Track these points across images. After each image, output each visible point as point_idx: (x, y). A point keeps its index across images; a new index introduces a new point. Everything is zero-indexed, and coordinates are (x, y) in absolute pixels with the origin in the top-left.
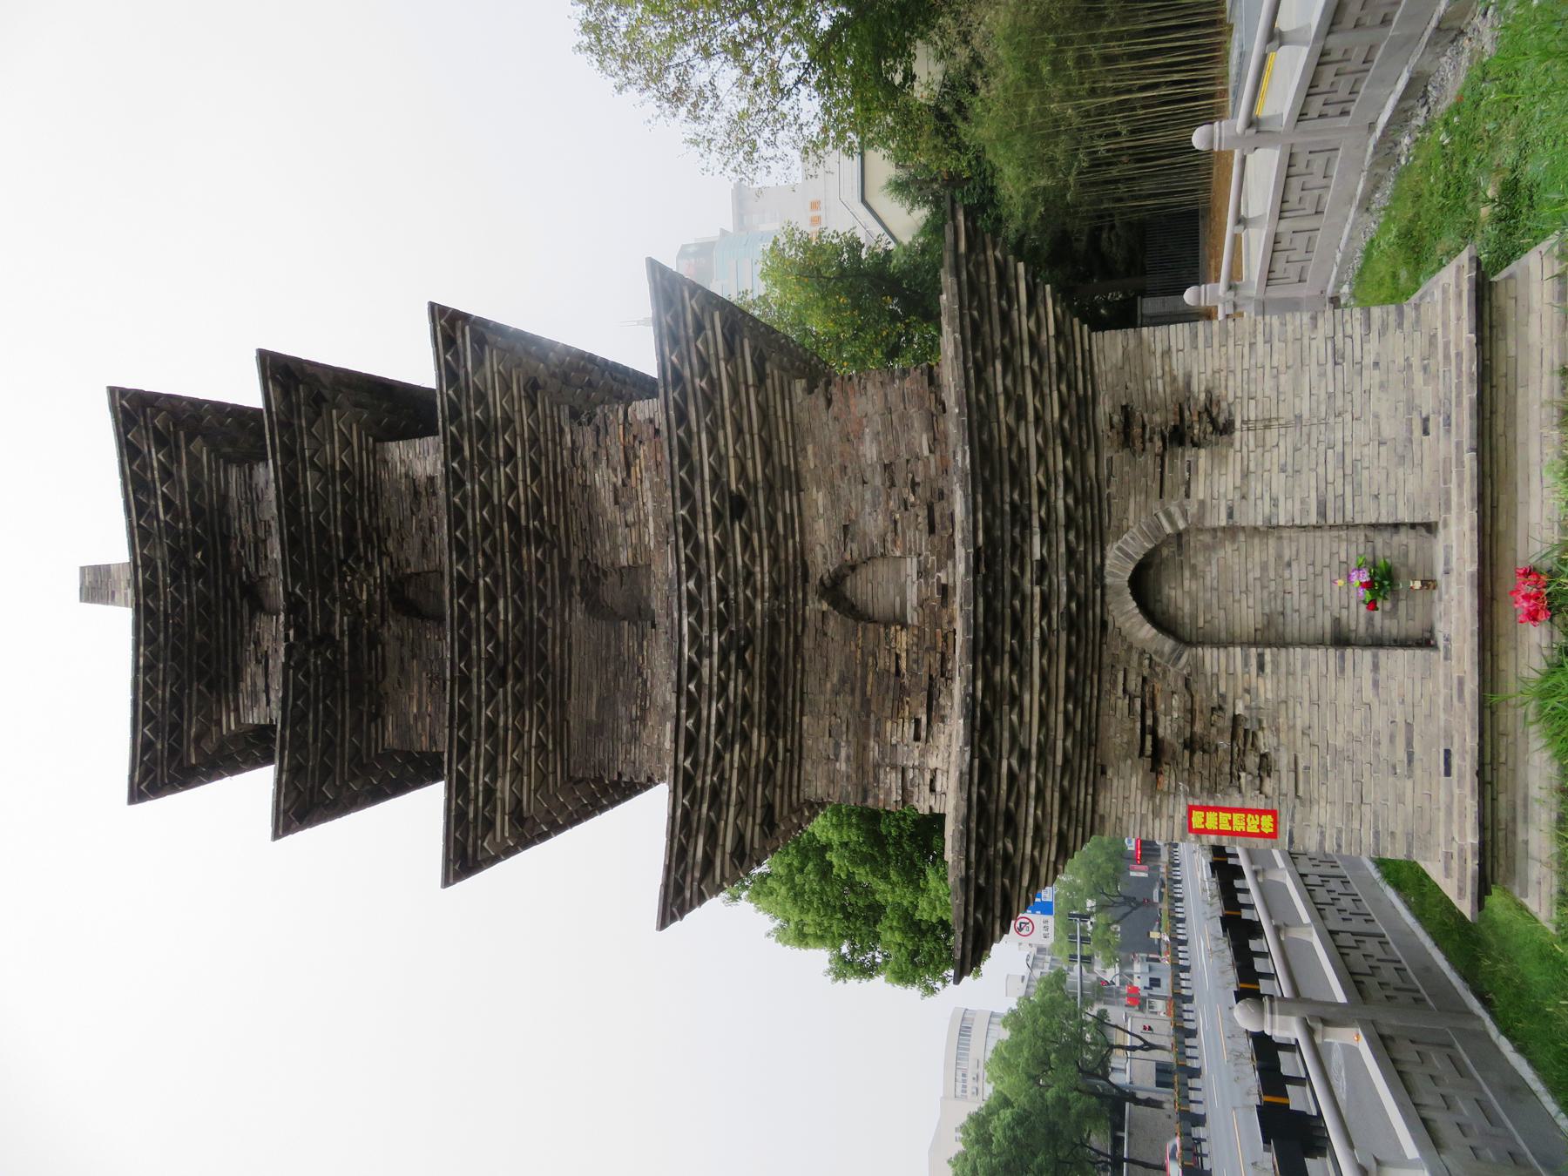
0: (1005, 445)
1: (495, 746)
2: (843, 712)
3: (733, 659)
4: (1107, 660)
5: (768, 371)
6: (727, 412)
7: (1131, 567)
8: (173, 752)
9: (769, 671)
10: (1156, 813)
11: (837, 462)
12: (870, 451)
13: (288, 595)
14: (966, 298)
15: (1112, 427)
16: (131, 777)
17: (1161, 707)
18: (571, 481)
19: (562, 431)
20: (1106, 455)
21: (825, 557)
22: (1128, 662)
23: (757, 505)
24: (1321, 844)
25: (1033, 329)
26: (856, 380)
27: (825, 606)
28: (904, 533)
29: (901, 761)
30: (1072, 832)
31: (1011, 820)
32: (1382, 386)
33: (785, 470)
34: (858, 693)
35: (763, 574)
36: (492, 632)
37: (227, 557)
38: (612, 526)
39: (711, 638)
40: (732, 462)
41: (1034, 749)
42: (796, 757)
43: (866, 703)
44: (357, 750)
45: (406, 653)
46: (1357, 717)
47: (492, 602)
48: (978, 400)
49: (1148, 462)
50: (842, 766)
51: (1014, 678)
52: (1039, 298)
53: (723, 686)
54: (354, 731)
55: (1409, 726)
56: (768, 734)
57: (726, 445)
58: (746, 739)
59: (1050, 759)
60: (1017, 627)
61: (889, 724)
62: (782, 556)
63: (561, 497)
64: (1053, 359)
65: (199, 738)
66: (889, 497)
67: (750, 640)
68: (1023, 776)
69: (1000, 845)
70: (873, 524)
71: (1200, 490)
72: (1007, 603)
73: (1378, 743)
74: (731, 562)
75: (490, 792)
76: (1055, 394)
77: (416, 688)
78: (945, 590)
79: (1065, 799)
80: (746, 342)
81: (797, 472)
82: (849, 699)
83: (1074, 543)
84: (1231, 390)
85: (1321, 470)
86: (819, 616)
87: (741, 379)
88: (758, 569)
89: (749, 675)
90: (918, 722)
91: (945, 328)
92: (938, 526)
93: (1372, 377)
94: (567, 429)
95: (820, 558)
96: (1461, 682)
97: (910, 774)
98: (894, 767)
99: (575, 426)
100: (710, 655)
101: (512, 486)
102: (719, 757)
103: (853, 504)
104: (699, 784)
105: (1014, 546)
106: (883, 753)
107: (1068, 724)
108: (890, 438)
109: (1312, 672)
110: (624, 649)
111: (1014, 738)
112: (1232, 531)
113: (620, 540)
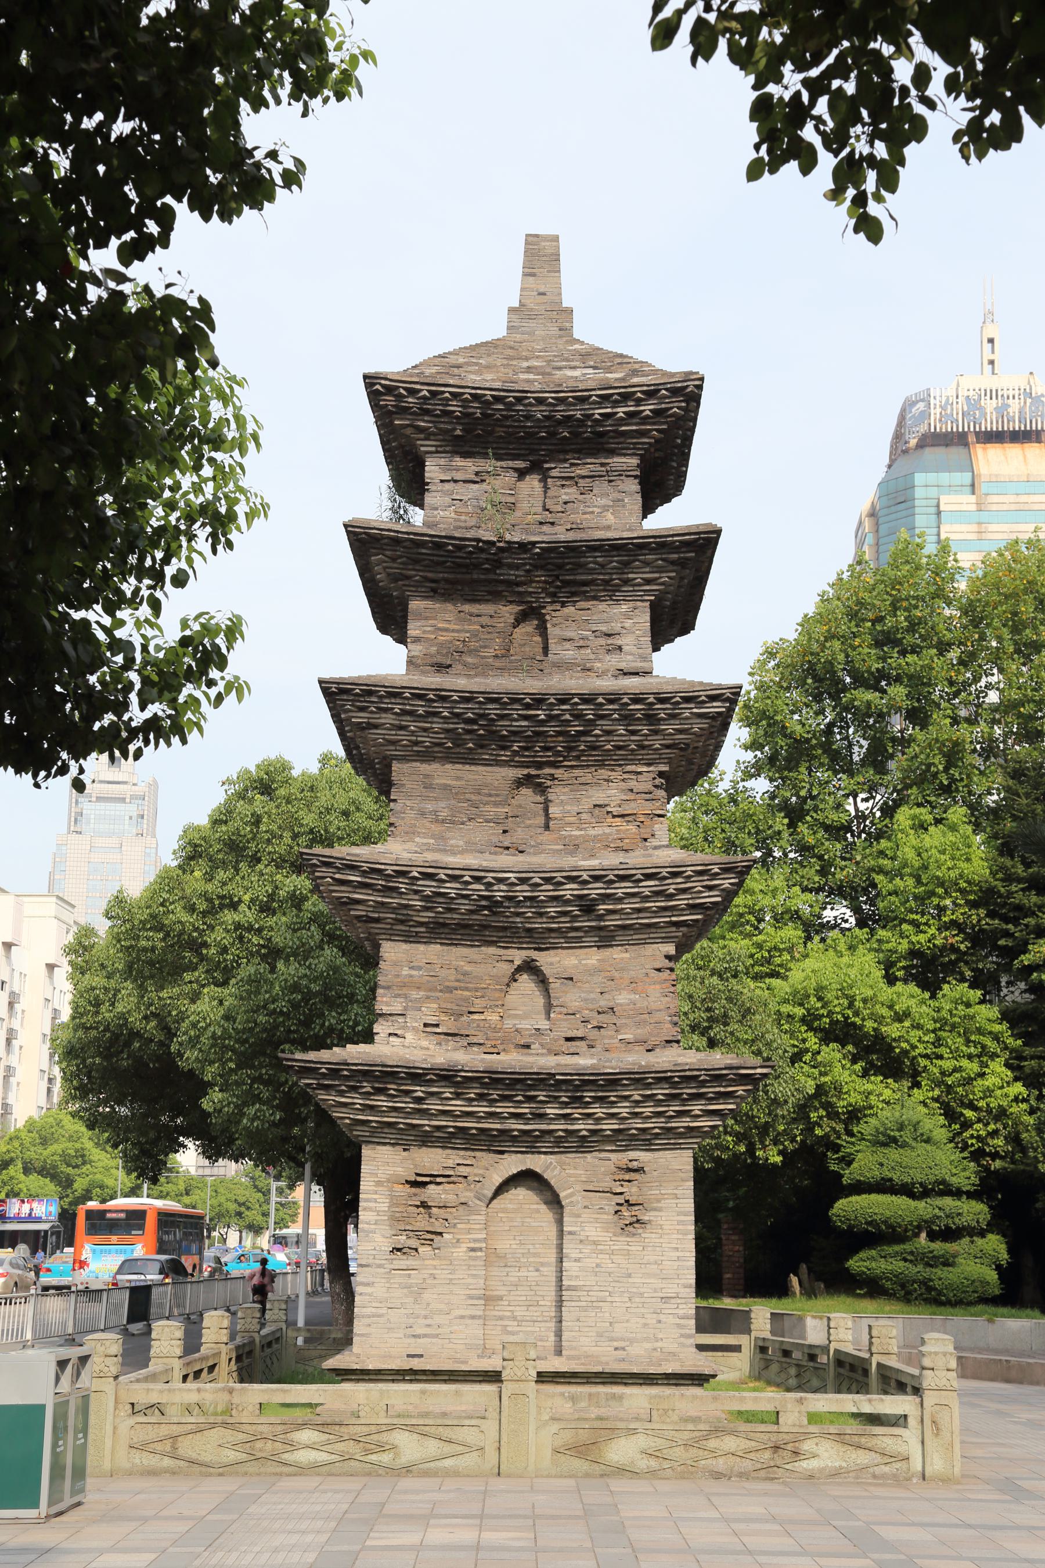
1: (420, 716)
3: (484, 903)
4: (478, 1154)
10: (379, 1183)
11: (616, 974)
12: (622, 998)
13: (534, 543)
16: (386, 379)
17: (447, 1187)
18: (613, 770)
19: (649, 765)
20: (613, 1156)
21: (552, 964)
26: (672, 989)
27: (517, 962)
31: (379, 1091)
32: (645, 1325)
34: (457, 984)
36: (502, 717)
37: (566, 452)
42: (410, 938)
43: (450, 990)
44: (408, 578)
45: (485, 620)
46: (442, 1306)
47: (526, 718)
49: (607, 1183)
50: (406, 971)
55: (437, 1336)
60: (504, 1098)
61: (436, 1006)
63: (601, 764)
65: (417, 428)
67: (495, 914)
71: (586, 1215)
73: (426, 1317)
77: (456, 627)
78: (528, 1047)
79: (390, 1125)
80: (699, 917)
81: (612, 946)
82: (452, 978)
84: (648, 1235)
85: (596, 1288)
89: (471, 912)
90: (437, 1026)
91: (701, 1055)
93: (651, 1319)
94: (651, 769)
95: (550, 960)
96: (465, 1362)
97: (401, 1019)
98: (406, 1008)
99: (653, 775)
100: (486, 890)
101: (608, 733)
102: (416, 892)
107: (438, 1128)
109: (471, 1281)
110: (488, 808)
112: (561, 1233)
113: (568, 808)
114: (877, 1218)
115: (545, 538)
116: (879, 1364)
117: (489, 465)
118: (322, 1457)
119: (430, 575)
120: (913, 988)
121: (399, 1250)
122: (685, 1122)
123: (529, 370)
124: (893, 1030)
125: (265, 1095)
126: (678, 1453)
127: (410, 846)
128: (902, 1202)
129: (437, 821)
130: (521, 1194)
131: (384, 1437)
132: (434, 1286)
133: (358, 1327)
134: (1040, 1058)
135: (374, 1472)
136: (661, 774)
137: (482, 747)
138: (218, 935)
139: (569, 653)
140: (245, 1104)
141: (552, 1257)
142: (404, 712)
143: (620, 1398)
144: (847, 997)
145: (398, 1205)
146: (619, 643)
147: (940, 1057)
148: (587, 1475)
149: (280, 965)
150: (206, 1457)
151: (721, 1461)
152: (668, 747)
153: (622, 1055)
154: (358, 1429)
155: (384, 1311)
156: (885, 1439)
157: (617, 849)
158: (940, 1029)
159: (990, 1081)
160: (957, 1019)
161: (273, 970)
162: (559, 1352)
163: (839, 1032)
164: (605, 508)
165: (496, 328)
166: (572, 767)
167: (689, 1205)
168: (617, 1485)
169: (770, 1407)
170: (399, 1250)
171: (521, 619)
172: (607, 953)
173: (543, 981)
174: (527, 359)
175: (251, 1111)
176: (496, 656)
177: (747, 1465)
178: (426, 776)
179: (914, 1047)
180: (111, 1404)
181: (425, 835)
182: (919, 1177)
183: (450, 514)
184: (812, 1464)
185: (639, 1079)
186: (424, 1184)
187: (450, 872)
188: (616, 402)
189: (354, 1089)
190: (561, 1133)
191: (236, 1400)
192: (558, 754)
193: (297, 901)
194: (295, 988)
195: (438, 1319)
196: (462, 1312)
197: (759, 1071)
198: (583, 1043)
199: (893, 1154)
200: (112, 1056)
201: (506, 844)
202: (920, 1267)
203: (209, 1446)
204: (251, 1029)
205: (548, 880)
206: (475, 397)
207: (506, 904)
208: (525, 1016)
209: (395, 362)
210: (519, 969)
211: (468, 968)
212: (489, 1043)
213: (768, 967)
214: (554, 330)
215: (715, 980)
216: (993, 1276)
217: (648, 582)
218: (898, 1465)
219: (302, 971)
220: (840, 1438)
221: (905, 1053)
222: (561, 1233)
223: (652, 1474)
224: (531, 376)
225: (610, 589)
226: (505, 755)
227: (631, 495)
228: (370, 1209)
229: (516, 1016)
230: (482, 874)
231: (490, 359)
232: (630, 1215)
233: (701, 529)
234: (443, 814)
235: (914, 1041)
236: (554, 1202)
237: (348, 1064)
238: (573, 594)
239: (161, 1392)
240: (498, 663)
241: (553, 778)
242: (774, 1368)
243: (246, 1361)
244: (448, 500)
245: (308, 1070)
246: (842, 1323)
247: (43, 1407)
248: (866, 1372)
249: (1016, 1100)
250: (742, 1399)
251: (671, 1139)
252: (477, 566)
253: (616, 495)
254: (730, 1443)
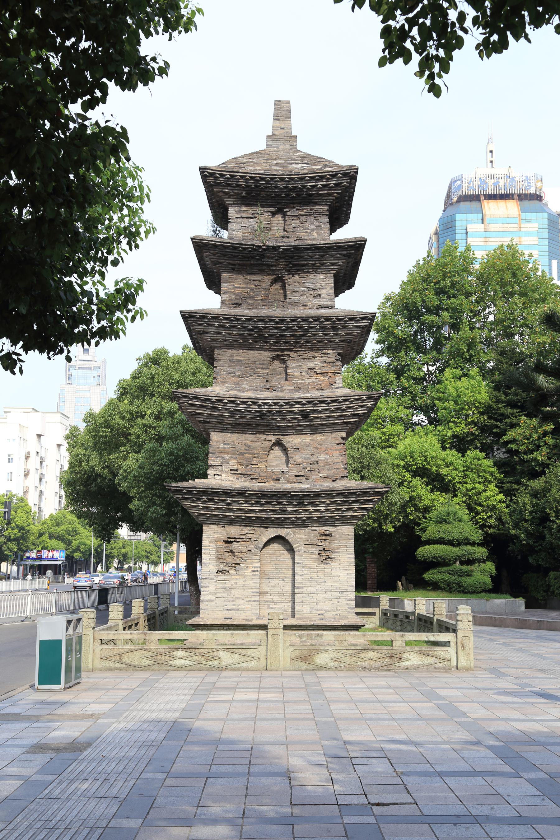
2: (239, 446)
3: (257, 414)
4: (256, 528)
8: (218, 184)
10: (211, 542)
11: (319, 446)
12: (322, 457)
19: (333, 350)
20: (317, 529)
24: (204, 587)
27: (273, 441)
32: (332, 604)
33: (317, 430)
36: (265, 328)
37: (294, 203)
38: (301, 367)
42: (223, 430)
43: (242, 454)
44: (221, 263)
46: (240, 596)
47: (276, 328)
49: (315, 541)
50: (222, 446)
54: (229, 263)
55: (238, 610)
58: (231, 417)
63: (311, 350)
65: (225, 193)
67: (263, 419)
71: (305, 555)
73: (233, 601)
75: (211, 325)
78: (278, 480)
79: (215, 515)
84: (333, 564)
89: (252, 418)
90: (236, 470)
91: (357, 483)
97: (220, 468)
98: (222, 463)
101: (314, 335)
102: (226, 409)
106: (227, 459)
107: (238, 517)
110: (259, 370)
112: (294, 564)
114: (437, 555)
115: (285, 244)
116: (437, 620)
117: (258, 210)
118: (187, 663)
119: (231, 262)
120: (454, 452)
121: (220, 571)
122: (350, 513)
123: (277, 165)
124: (445, 471)
125: (158, 502)
126: (347, 659)
127: (223, 388)
128: (448, 548)
129: (235, 376)
130: (275, 546)
131: (215, 654)
132: (237, 587)
133: (202, 606)
134: (511, 482)
135: (210, 669)
136: (339, 354)
137: (256, 342)
138: (136, 430)
139: (296, 298)
140: (149, 506)
141: (290, 574)
142: (220, 326)
143: (321, 636)
144: (424, 456)
145: (219, 552)
146: (319, 293)
147: (466, 483)
148: (306, 670)
149: (164, 444)
150: (135, 663)
151: (366, 662)
152: (342, 341)
153: (322, 483)
154: (203, 650)
155: (214, 599)
156: (440, 652)
157: (319, 389)
158: (466, 470)
159: (489, 493)
160: (474, 466)
161: (161, 445)
162: (293, 616)
163: (420, 472)
164: (312, 230)
165: (261, 145)
166: (298, 351)
167: (352, 550)
168: (320, 673)
169: (389, 639)
170: (220, 571)
171: (274, 282)
172: (314, 436)
173: (285, 450)
174: (276, 160)
175: (152, 509)
176: (262, 300)
177: (378, 664)
178: (231, 356)
179: (454, 479)
180: (92, 640)
181: (230, 383)
182: (456, 537)
183: (240, 233)
184: (407, 663)
185: (329, 494)
186: (231, 542)
188: (318, 180)
189: (199, 499)
191: (148, 638)
192: (291, 345)
193: (171, 414)
194: (171, 454)
195: (238, 602)
196: (250, 599)
197: (384, 489)
198: (304, 478)
199: (445, 527)
200: (88, 485)
201: (268, 387)
202: (456, 577)
203: (137, 658)
204: (151, 473)
205: (287, 403)
206: (252, 178)
208: (277, 466)
209: (214, 161)
210: (274, 444)
212: (261, 478)
213: (388, 443)
214: (288, 146)
215: (364, 449)
216: (489, 580)
217: (333, 264)
218: (446, 663)
219: (174, 446)
220: (420, 652)
221: (450, 481)
222: (294, 564)
223: (336, 669)
224: (278, 168)
225: (315, 268)
226: (267, 346)
227: (325, 223)
228: (207, 554)
229: (272, 466)
231: (258, 160)
232: (326, 556)
233: (357, 239)
234: (238, 373)
235: (454, 476)
236: (291, 549)
238: (298, 270)
239: (114, 634)
240: (263, 303)
241: (289, 356)
242: (390, 622)
243: (152, 621)
244: (239, 226)
245: (178, 491)
246: (421, 602)
247: (61, 641)
248: (432, 623)
249: (500, 502)
250: (376, 636)
251: (343, 520)
252: (253, 258)
253: (317, 224)
254: (371, 655)
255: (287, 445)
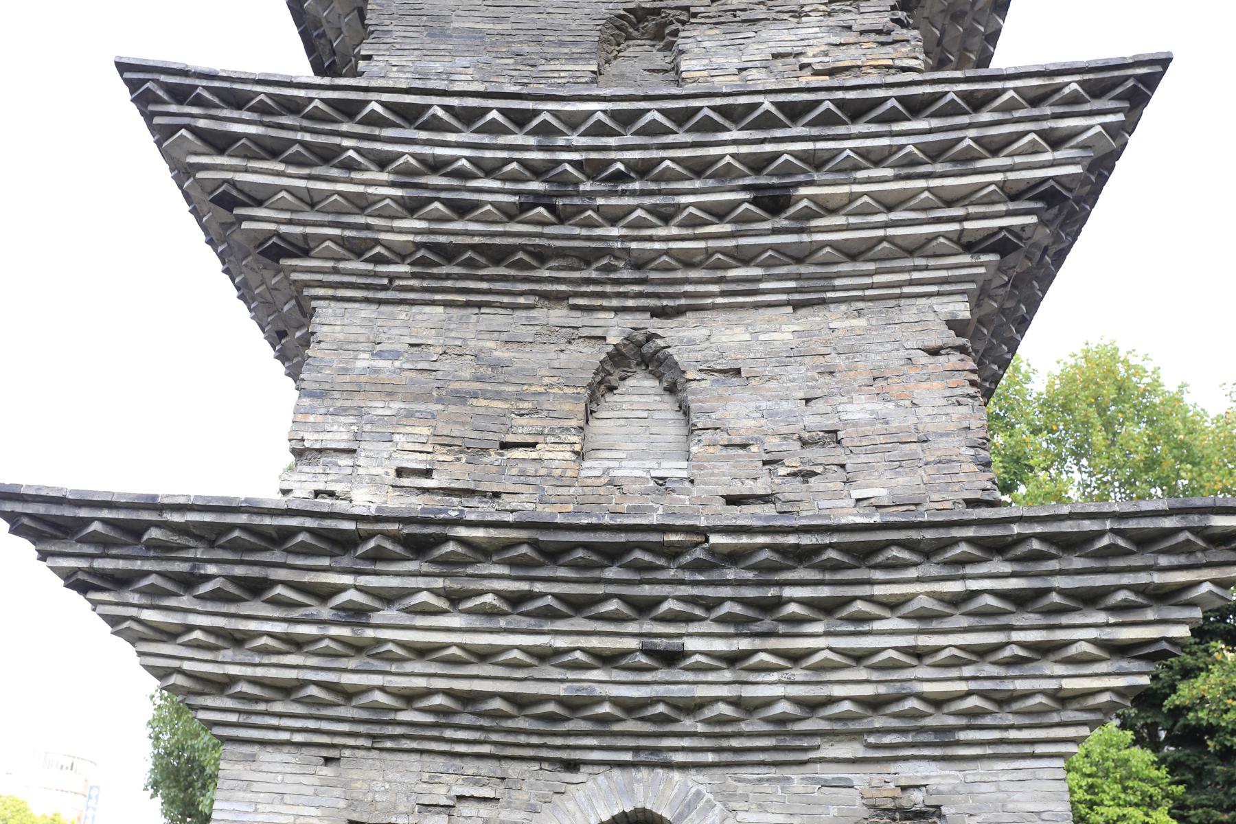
0: (879, 590)
3: (536, 186)
4: (514, 770)
5: (984, 258)
6: (921, 183)
7: (666, 813)
9: (514, 249)
11: (839, 362)
12: (858, 410)
14: (1132, 524)
15: (904, 788)
21: (691, 342)
22: (509, 805)
23: (775, 231)
25: (1072, 651)
27: (614, 339)
28: (728, 459)
29: (365, 447)
30: (229, 703)
34: (478, 386)
35: (666, 238)
39: (568, 148)
40: (845, 189)
41: (370, 633)
42: (379, 293)
43: (461, 397)
48: (955, 542)
51: (489, 598)
52: (1125, 665)
53: (490, 169)
56: (419, 246)
57: (869, 181)
59: (352, 664)
61: (426, 431)
62: (693, 274)
64: (1020, 685)
66: (785, 437)
67: (561, 217)
68: (325, 613)
69: (211, 569)
70: (739, 411)
72: (611, 589)
74: (686, 185)
76: (962, 687)
79: (286, 690)
81: (823, 302)
82: (467, 374)
83: (708, 713)
86: (598, 332)
87: (972, 210)
88: (674, 231)
89: (511, 213)
90: (427, 473)
92: (735, 510)
95: (687, 334)
97: (345, 461)
98: (357, 438)
103: (773, 385)
104: (344, 127)
105: (710, 605)
107: (410, 698)
108: (881, 439)
111: (388, 598)
122: (1055, 675)
147: (1101, 804)
187: (455, 102)
190: (724, 709)
207: (586, 187)
210: (617, 358)
211: (501, 354)
230: (529, 105)
237: (162, 508)
255: (680, 355)
